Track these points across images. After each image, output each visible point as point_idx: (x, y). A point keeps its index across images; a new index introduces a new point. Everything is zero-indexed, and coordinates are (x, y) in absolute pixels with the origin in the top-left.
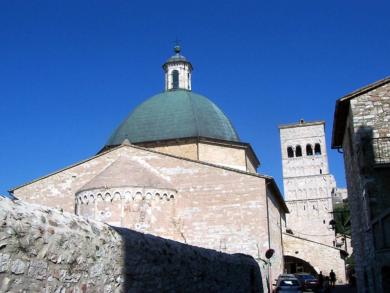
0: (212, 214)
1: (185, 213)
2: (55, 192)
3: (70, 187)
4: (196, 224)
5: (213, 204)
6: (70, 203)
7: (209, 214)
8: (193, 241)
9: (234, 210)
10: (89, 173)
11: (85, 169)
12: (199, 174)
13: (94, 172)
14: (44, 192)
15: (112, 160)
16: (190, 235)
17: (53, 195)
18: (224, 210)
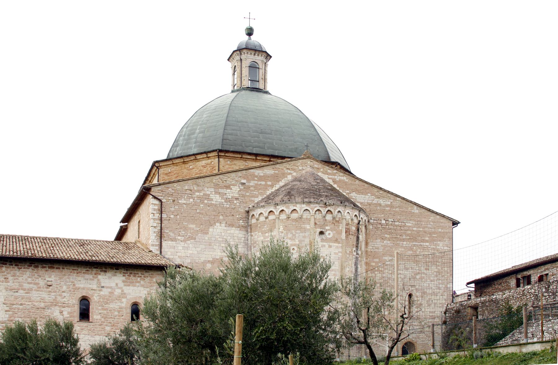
0: (403, 249)
1: (376, 246)
2: (217, 199)
3: (237, 195)
4: (386, 258)
5: (404, 240)
6: (238, 216)
7: (400, 249)
8: (384, 275)
9: (424, 248)
10: (263, 183)
11: (256, 177)
12: (391, 206)
13: (269, 183)
14: (199, 197)
15: (292, 172)
16: (380, 269)
17: (213, 202)
18: (415, 248)
